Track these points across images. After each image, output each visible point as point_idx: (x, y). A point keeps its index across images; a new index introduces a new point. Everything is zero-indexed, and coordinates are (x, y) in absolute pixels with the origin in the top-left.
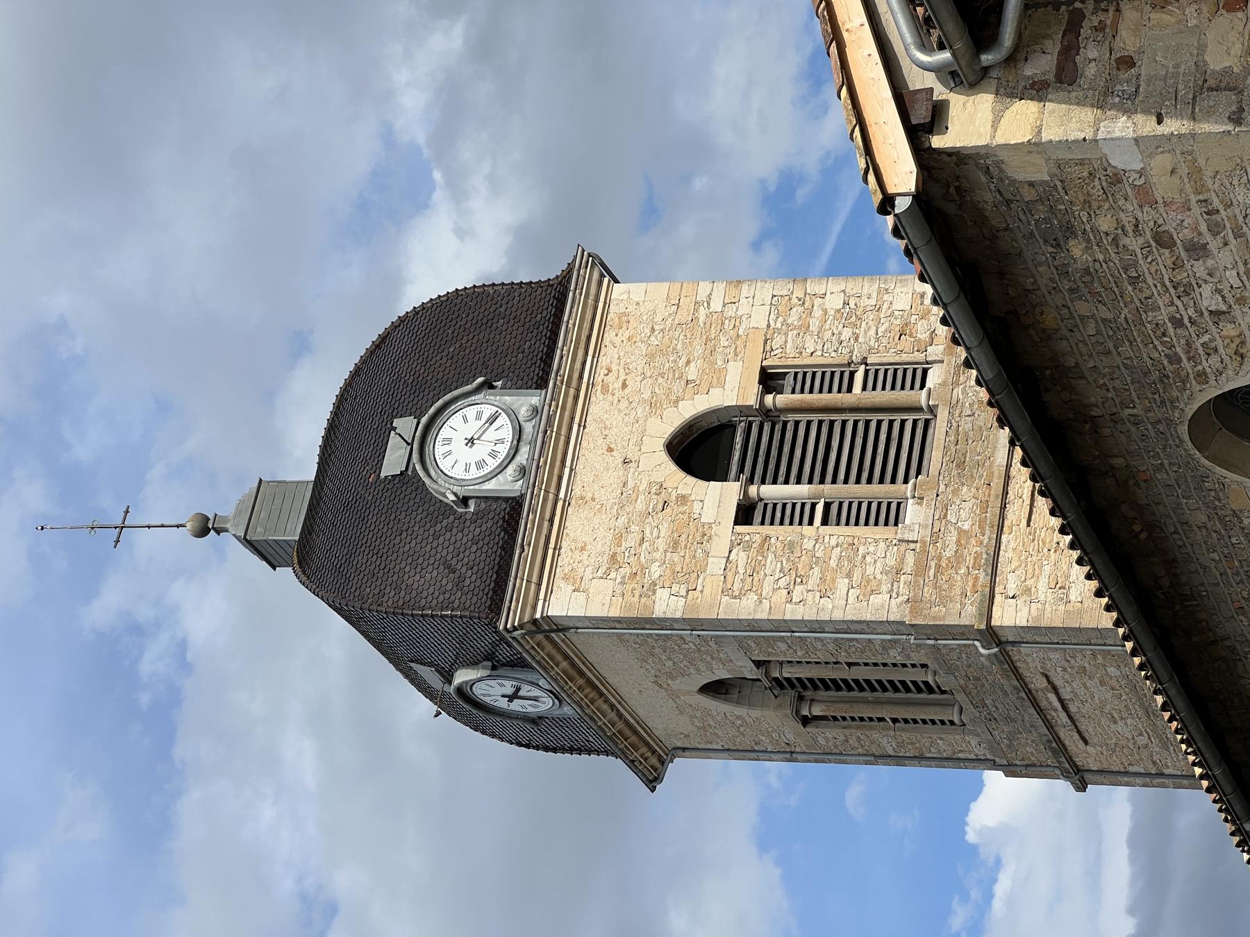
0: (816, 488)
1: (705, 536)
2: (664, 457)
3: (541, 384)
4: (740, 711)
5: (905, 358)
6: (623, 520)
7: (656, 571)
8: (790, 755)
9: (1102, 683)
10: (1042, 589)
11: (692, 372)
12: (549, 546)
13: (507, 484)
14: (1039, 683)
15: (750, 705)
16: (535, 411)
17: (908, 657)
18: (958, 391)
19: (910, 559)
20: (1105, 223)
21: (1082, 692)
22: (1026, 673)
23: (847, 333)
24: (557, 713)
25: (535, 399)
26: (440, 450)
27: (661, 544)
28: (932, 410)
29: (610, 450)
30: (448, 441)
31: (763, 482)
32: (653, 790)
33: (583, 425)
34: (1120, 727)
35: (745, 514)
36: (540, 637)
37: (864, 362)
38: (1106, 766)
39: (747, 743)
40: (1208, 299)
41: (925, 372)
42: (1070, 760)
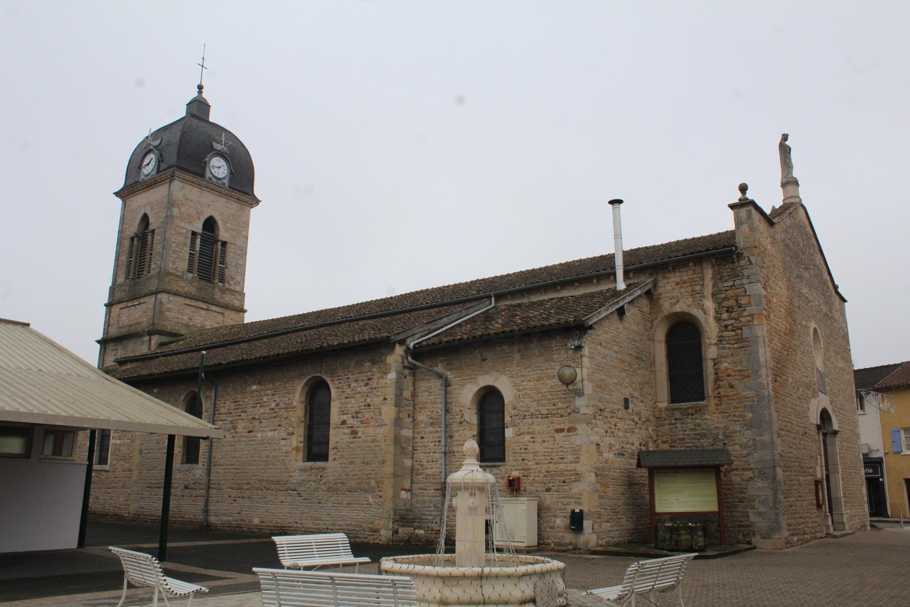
0: (198, 252)
1: (190, 223)
2: (209, 215)
3: (230, 187)
4: (137, 222)
5: (226, 278)
6: (196, 202)
7: (183, 209)
8: (121, 232)
9: (141, 316)
10: (169, 306)
11: (228, 225)
12: (192, 183)
13: (208, 175)
14: (142, 301)
15: (139, 225)
16: (224, 184)
17: (153, 269)
18: (217, 290)
19: (180, 274)
20: (374, 370)
21: (138, 310)
22: (145, 298)
23: (233, 264)
24: (142, 174)
25: (227, 184)
26: (218, 158)
27: (189, 212)
28: (213, 283)
29: (213, 202)
30: (220, 161)
31: (201, 239)
32: (114, 193)
33: (219, 196)
34: (125, 318)
35: (194, 234)
36: (169, 177)
37: (226, 268)
38: (112, 312)
39: (126, 221)
40: (353, 385)
41: (221, 282)
42: (115, 304)
